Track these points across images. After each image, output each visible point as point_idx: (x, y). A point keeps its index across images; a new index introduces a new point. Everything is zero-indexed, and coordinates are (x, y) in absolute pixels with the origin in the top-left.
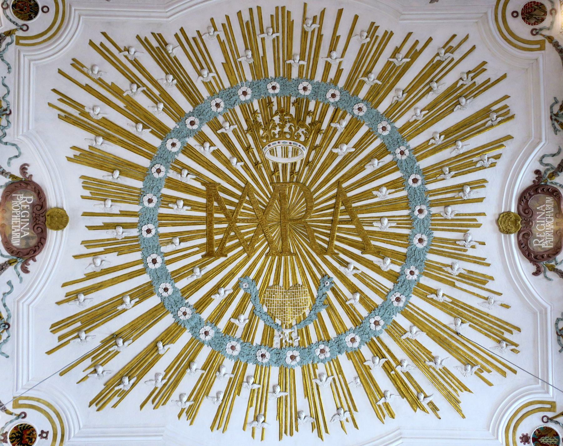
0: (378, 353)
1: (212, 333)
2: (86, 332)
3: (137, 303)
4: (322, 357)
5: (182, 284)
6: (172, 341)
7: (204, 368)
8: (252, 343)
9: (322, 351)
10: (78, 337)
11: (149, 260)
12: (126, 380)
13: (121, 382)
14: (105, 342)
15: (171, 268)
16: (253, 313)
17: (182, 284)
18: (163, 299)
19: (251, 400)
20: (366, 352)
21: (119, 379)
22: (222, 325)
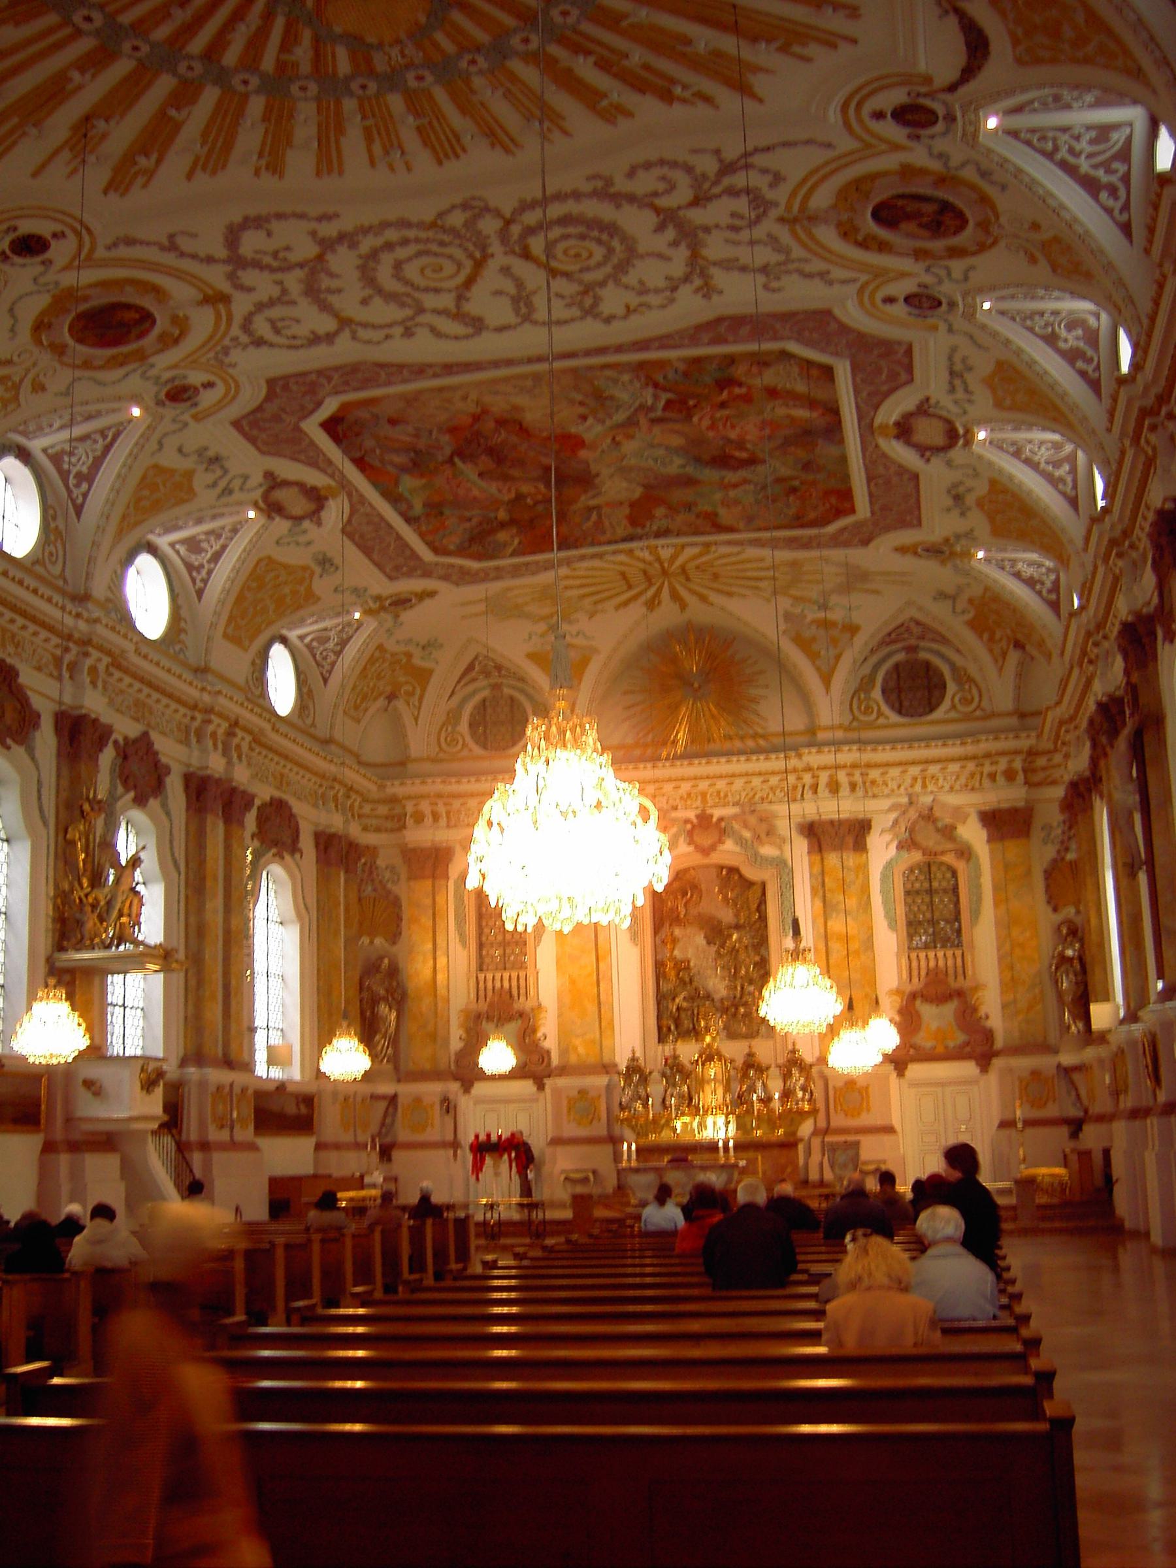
0: (577, 49)
1: (255, 81)
2: (34, 125)
3: (94, 76)
4: (473, 69)
5: (162, 32)
6: (193, 100)
7: (266, 118)
8: (335, 73)
9: (473, 62)
10: (24, 134)
11: (77, 18)
12: (143, 162)
13: (136, 164)
14: (75, 128)
15: (126, 19)
16: (317, 41)
17: (162, 32)
18: (140, 60)
19: (369, 138)
20: (554, 50)
21: (128, 159)
22: (268, 63)
